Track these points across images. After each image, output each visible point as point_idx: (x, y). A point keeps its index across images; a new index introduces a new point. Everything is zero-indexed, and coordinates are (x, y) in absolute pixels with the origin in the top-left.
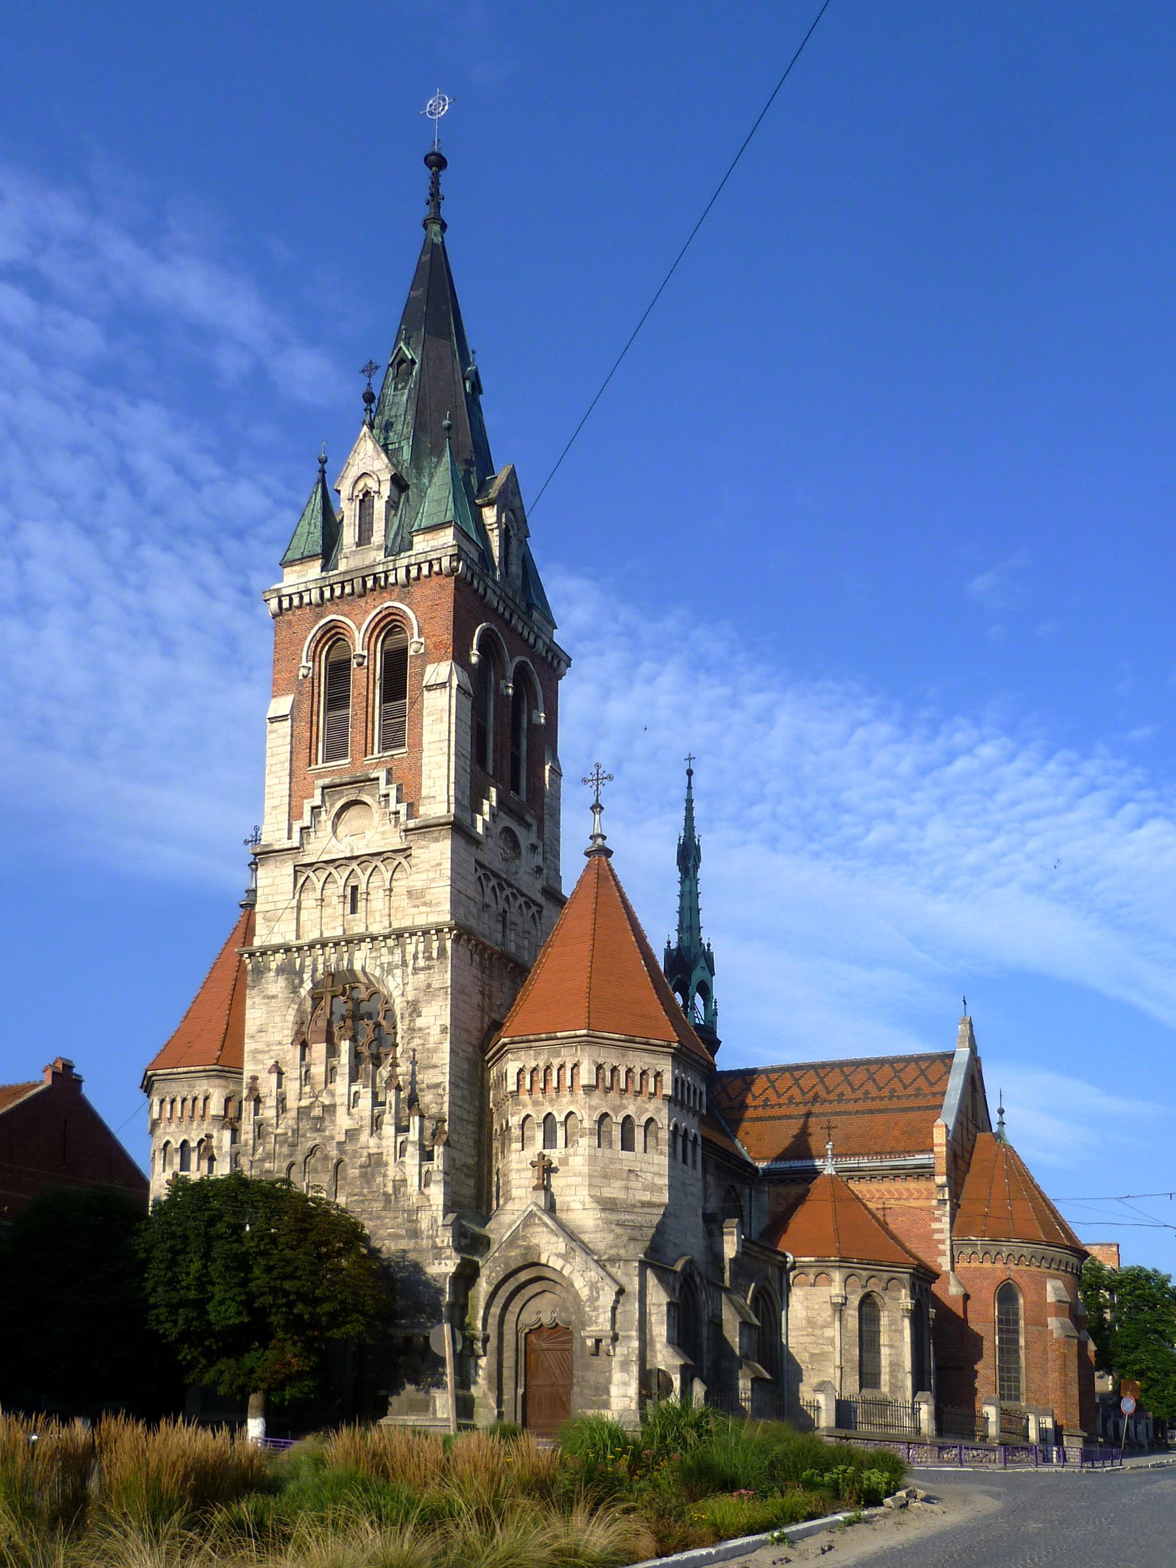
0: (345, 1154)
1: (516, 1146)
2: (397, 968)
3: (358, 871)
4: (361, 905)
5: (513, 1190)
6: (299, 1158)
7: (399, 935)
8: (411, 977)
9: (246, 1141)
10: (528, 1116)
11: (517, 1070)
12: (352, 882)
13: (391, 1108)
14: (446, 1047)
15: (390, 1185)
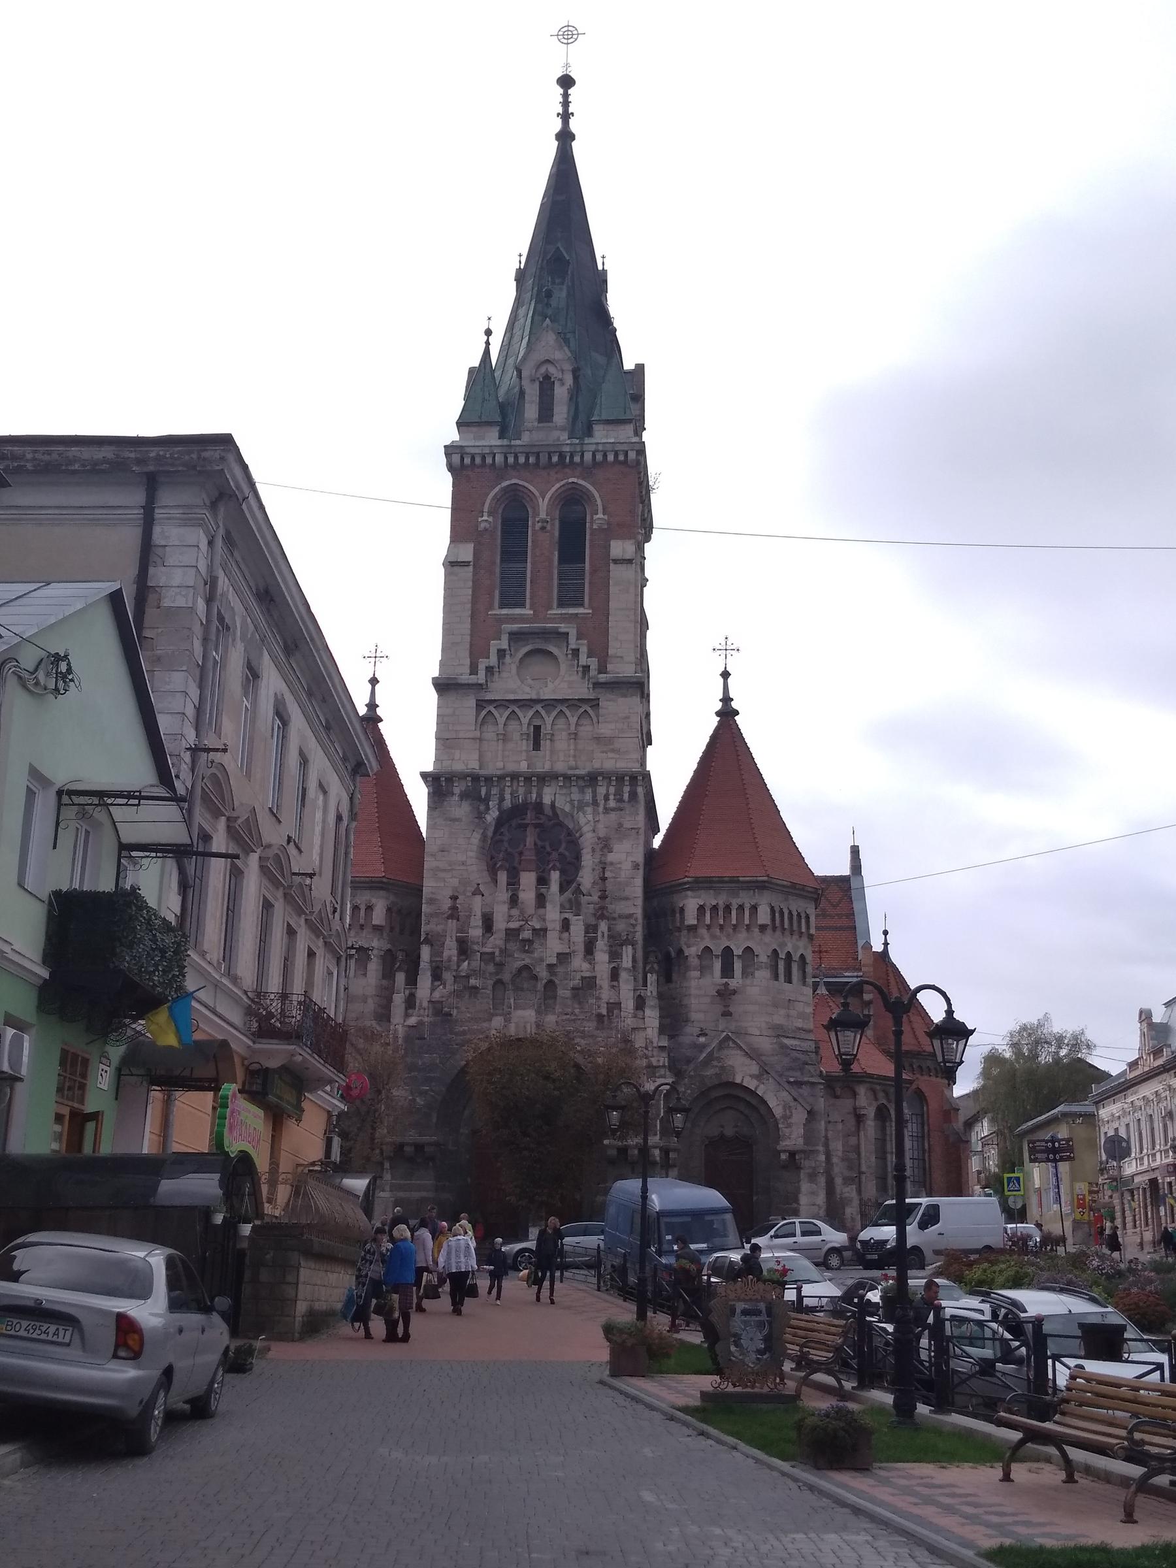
0: (556, 975)
1: (697, 974)
2: (588, 806)
3: (543, 713)
4: (545, 744)
5: (693, 1013)
6: (506, 977)
7: (592, 779)
8: (601, 817)
9: (449, 960)
10: (707, 949)
11: (698, 906)
12: (537, 722)
13: (603, 936)
14: (639, 881)
15: (606, 1006)
